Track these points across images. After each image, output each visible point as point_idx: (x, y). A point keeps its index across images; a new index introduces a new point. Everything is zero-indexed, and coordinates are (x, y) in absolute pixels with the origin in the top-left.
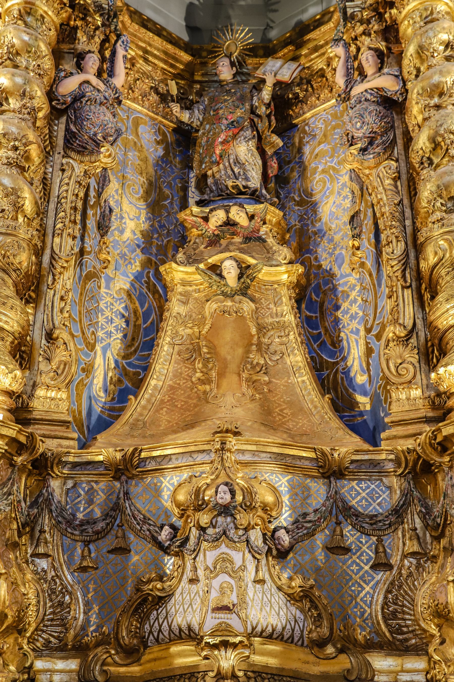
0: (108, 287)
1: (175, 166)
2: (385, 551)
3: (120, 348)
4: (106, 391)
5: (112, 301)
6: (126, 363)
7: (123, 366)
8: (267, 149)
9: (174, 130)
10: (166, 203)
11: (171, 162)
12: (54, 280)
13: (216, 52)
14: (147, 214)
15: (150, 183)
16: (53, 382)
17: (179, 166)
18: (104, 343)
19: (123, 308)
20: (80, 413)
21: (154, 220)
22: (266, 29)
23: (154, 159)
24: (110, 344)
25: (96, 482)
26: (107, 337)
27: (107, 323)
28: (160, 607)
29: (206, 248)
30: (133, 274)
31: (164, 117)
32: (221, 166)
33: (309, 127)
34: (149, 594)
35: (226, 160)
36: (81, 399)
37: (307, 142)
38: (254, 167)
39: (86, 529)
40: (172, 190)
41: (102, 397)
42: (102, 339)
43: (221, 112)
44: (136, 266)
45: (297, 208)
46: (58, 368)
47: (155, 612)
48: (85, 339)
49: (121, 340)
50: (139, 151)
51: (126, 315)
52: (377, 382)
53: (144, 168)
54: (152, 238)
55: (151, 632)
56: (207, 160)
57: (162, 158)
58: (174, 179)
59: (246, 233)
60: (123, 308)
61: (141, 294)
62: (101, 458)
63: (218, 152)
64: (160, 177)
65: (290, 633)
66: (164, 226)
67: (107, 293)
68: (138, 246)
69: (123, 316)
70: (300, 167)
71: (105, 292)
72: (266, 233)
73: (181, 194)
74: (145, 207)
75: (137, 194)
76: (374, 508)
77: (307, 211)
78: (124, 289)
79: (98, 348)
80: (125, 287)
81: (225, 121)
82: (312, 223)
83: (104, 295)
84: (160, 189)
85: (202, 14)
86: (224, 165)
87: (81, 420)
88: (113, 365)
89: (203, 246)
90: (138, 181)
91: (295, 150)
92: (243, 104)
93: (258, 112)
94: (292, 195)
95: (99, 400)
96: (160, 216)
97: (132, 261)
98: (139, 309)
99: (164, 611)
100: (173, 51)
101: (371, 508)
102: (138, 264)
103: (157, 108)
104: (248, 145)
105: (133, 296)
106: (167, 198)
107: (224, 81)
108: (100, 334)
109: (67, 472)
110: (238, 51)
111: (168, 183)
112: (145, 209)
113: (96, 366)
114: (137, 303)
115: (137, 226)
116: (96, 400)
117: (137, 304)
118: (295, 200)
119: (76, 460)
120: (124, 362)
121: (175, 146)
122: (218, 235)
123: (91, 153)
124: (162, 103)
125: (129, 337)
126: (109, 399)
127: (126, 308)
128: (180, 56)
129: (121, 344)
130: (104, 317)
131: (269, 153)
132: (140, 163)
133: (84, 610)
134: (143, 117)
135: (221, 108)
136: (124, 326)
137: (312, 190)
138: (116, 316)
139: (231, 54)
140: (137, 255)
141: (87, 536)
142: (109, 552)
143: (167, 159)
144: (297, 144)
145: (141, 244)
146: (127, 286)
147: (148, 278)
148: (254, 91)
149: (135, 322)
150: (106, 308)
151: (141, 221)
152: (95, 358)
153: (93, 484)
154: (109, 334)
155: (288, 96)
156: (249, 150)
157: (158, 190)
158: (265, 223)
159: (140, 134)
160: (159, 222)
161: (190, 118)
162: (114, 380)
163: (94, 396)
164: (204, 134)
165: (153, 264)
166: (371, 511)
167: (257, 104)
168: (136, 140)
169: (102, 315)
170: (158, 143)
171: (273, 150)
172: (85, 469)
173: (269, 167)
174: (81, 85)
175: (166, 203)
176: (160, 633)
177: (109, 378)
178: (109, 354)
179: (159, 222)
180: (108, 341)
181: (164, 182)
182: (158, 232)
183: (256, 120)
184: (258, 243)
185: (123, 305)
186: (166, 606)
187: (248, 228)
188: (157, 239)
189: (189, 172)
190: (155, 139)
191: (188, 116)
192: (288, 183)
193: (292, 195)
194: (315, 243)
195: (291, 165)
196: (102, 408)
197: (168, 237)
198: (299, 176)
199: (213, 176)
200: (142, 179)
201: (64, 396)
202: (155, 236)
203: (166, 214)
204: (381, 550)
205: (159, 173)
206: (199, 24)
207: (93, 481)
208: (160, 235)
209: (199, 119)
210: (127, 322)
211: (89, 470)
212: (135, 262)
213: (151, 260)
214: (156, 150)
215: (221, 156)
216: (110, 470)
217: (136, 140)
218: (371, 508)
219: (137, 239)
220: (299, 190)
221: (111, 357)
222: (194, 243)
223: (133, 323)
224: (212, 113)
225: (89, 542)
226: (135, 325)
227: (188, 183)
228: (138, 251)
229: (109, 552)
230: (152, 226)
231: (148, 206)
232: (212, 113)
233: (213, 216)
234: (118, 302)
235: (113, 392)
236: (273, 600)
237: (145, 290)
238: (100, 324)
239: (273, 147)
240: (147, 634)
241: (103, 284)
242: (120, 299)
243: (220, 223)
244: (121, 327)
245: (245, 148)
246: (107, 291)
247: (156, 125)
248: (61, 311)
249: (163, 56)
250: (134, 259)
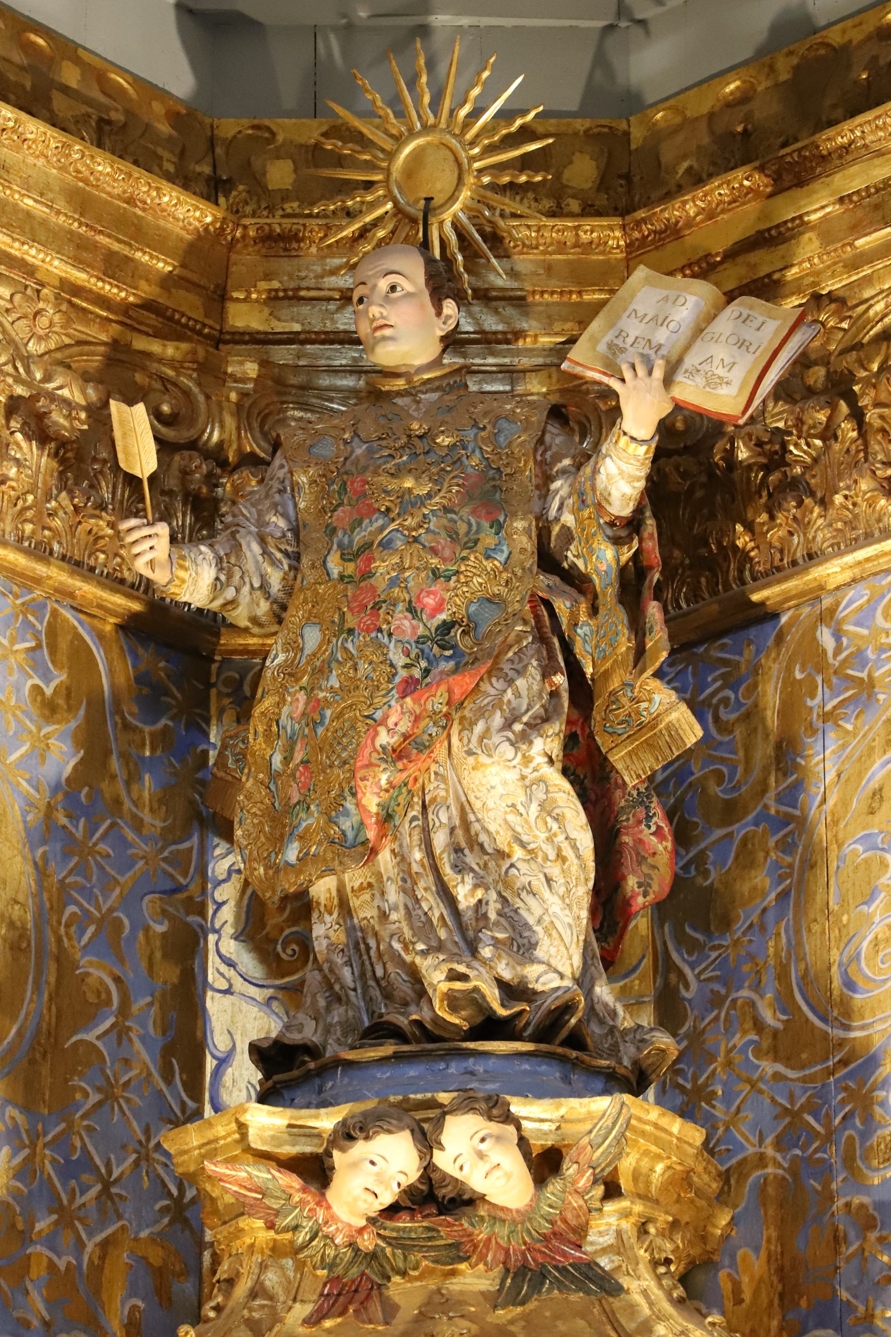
1: (138, 825)
8: (617, 759)
10: (90, 1036)
13: (340, 161)
17: (153, 822)
22: (610, 28)
29: (313, 1320)
31: (76, 566)
32: (385, 858)
33: (838, 635)
35: (406, 828)
37: (826, 717)
38: (554, 871)
40: (121, 961)
43: (383, 567)
45: (768, 1067)
54: (25, 1237)
56: (310, 820)
58: (130, 901)
59: (516, 1245)
63: (372, 802)
66: (86, 1162)
70: (787, 847)
72: (619, 1247)
73: (170, 974)
77: (822, 1094)
81: (403, 622)
82: (849, 1161)
84: (64, 962)
86: (401, 858)
89: (302, 1310)
91: (763, 751)
92: (499, 527)
93: (572, 556)
94: (745, 993)
103: (42, 518)
104: (527, 760)
107: (394, 374)
110: (465, 194)
118: (759, 1025)
122: (373, 1256)
131: (631, 782)
135: (386, 545)
137: (850, 985)
139: (429, 208)
143: (95, 793)
144: (772, 719)
148: (556, 437)
155: (730, 454)
156: (528, 785)
158: (612, 1191)
160: (61, 1143)
161: (218, 586)
164: (291, 672)
167: (568, 519)
171: (650, 763)
173: (629, 859)
175: (90, 1036)
179: (61, 1143)
181: (81, 921)
183: (562, 606)
184: (576, 1297)
187: (527, 1215)
188: (51, 1241)
189: (204, 852)
190: (36, 689)
191: (207, 574)
192: (726, 923)
193: (745, 993)
194: (862, 1273)
195: (740, 829)
197: (103, 1224)
198: (783, 896)
199: (345, 908)
202: (42, 1225)
209: (264, 587)
214: (41, 752)
215: (386, 818)
220: (783, 975)
222: (253, 1294)
224: (335, 565)
227: (202, 913)
230: (25, 1172)
232: (335, 565)
233: (355, 1165)
239: (650, 745)
243: (387, 1198)
245: (512, 776)
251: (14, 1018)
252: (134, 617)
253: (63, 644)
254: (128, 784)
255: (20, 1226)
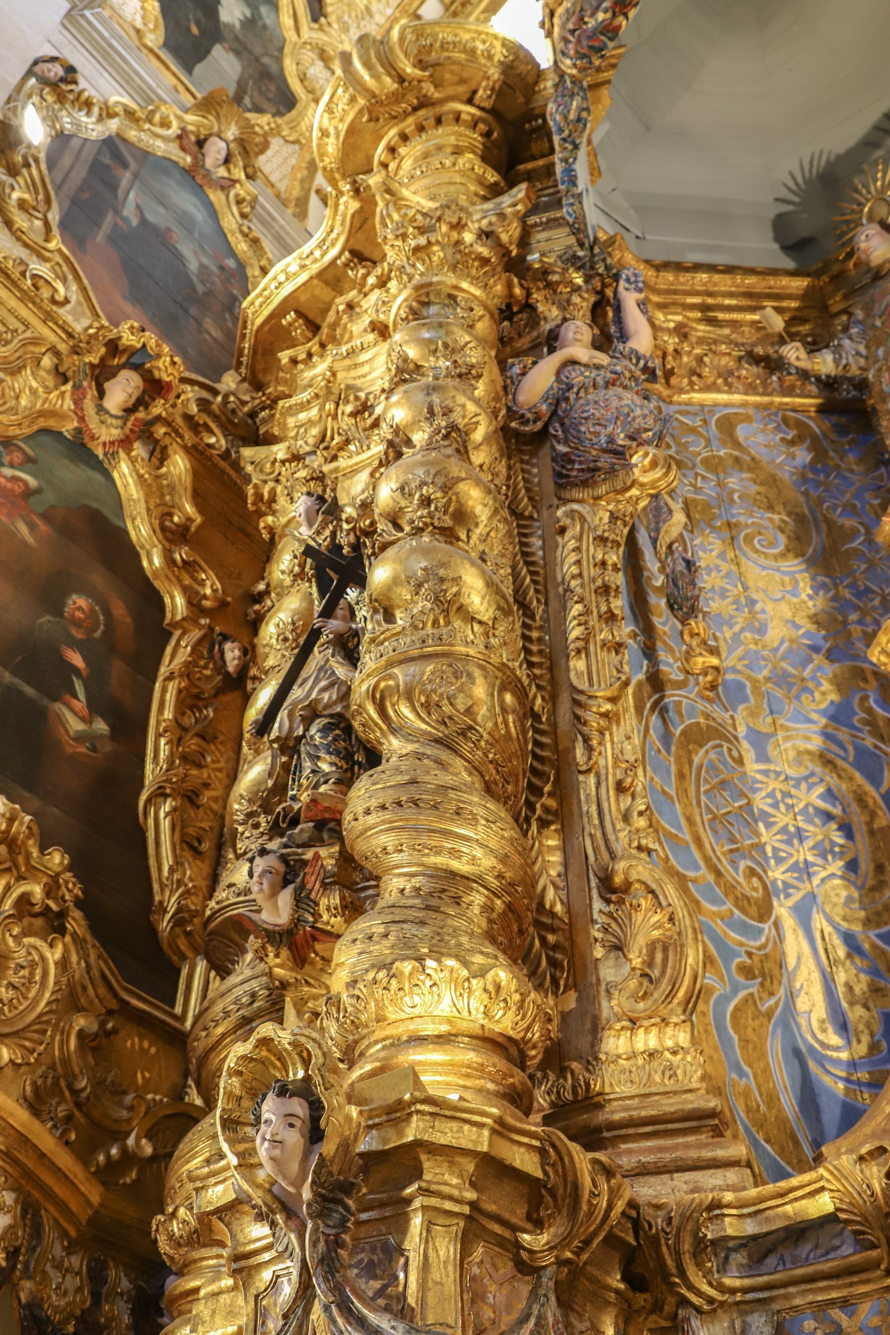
0: (762, 757)
3: (849, 900)
4: (843, 1027)
5: (785, 787)
6: (880, 936)
7: (874, 946)
9: (821, 410)
11: (838, 467)
12: (590, 749)
14: (813, 578)
15: (800, 519)
16: (641, 1005)
18: (797, 896)
19: (821, 797)
20: (772, 1099)
21: (836, 586)
23: (792, 474)
24: (813, 896)
25: (845, 1304)
26: (800, 879)
27: (789, 842)
30: (823, 713)
36: (763, 1056)
41: (837, 1049)
42: (786, 885)
44: (823, 694)
46: (650, 963)
48: (730, 889)
49: (842, 878)
50: (750, 470)
51: (837, 811)
53: (772, 495)
54: (845, 623)
57: (812, 466)
60: (821, 797)
61: (861, 752)
62: (824, 1204)
64: (821, 501)
67: (765, 773)
68: (815, 649)
69: (829, 817)
71: (761, 772)
74: (803, 567)
75: (775, 547)
78: (808, 752)
79: (782, 910)
80: (811, 747)
83: (759, 777)
84: (830, 523)
85: (805, 216)
87: (782, 1122)
88: (841, 952)
90: (766, 523)
95: (831, 1059)
96: (851, 573)
97: (811, 685)
98: (869, 788)
100: (763, 284)
102: (826, 686)
105: (840, 762)
106: (854, 533)
108: (777, 874)
109: (737, 1283)
111: (844, 506)
112: (806, 570)
113: (791, 961)
114: (858, 776)
115: (796, 609)
116: (821, 1060)
117: (859, 778)
119: (750, 1228)
120: (872, 934)
121: (834, 436)
123: (612, 472)
124: (772, 373)
125: (866, 865)
126: (862, 1049)
127: (830, 795)
128: (783, 287)
129: (846, 887)
130: (776, 829)
132: (761, 489)
134: (740, 411)
136: (841, 841)
138: (810, 821)
140: (819, 668)
145: (822, 643)
146: (816, 743)
147: (869, 711)
149: (869, 823)
150: (775, 806)
151: (804, 596)
152: (781, 938)
153: (836, 1314)
154: (805, 871)
157: (824, 527)
159: (741, 440)
162: (857, 990)
163: (811, 1048)
165: (870, 677)
168: (736, 453)
169: (768, 825)
170: (792, 443)
172: (796, 1262)
174: (558, 373)
175: (854, 545)
177: (841, 990)
178: (819, 922)
180: (806, 887)
182: (856, 608)
185: (820, 790)
188: (860, 622)
190: (782, 439)
196: (847, 1080)
200: (776, 517)
201: (683, 1038)
202: (853, 617)
203: (864, 567)
205: (814, 494)
206: (804, 231)
207: (832, 1303)
208: (864, 613)
210: (847, 829)
211: (807, 1262)
212: (819, 684)
213: (862, 670)
216: (874, 1246)
217: (736, 453)
219: (807, 635)
221: (828, 929)
223: (864, 828)
226: (872, 833)
228: (818, 658)
231: (811, 563)
234: (804, 786)
235: (868, 1025)
237: (869, 742)
238: (769, 849)
241: (749, 755)
242: (806, 778)
244: (833, 844)
246: (762, 767)
247: (776, 414)
248: (626, 818)
249: (744, 302)
250: (814, 678)
251: (809, 545)
252: (821, 405)
253: (791, 422)
254: (841, 459)
255: (840, 618)
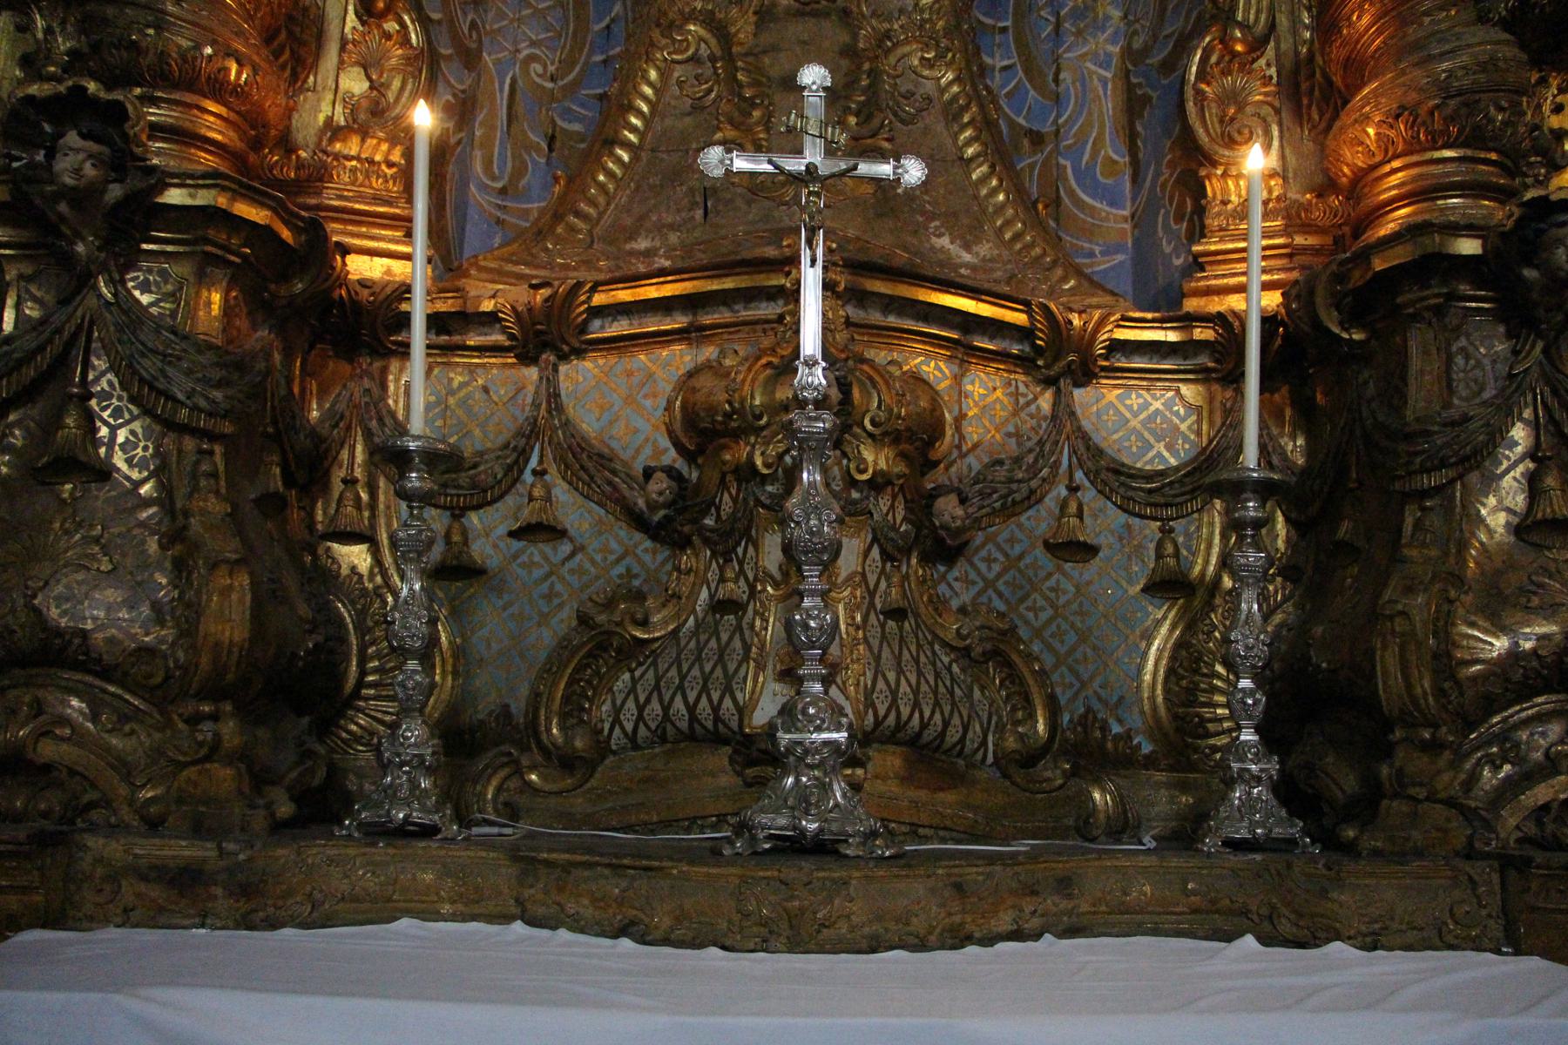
2: (1177, 554)
28: (640, 664)
34: (610, 634)
39: (454, 480)
47: (627, 676)
52: (1157, 174)
55: (616, 721)
65: (958, 736)
76: (1159, 455)
99: (651, 674)
101: (1151, 455)
133: (454, 666)
141: (459, 496)
142: (512, 534)
166: (1151, 461)
176: (641, 725)
186: (655, 664)
204: (1170, 549)
218: (1151, 455)
225: (465, 510)
229: (512, 534)
236: (923, 659)
240: (607, 726)
